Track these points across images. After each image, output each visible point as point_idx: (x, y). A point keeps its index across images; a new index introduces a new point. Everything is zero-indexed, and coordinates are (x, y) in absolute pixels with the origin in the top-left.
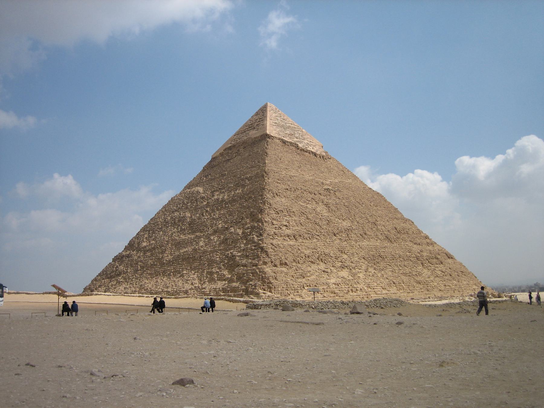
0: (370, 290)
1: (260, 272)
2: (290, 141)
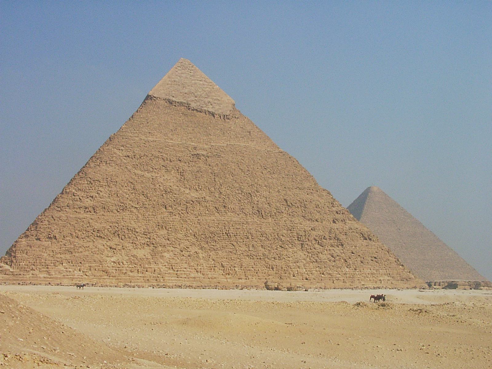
0: (171, 271)
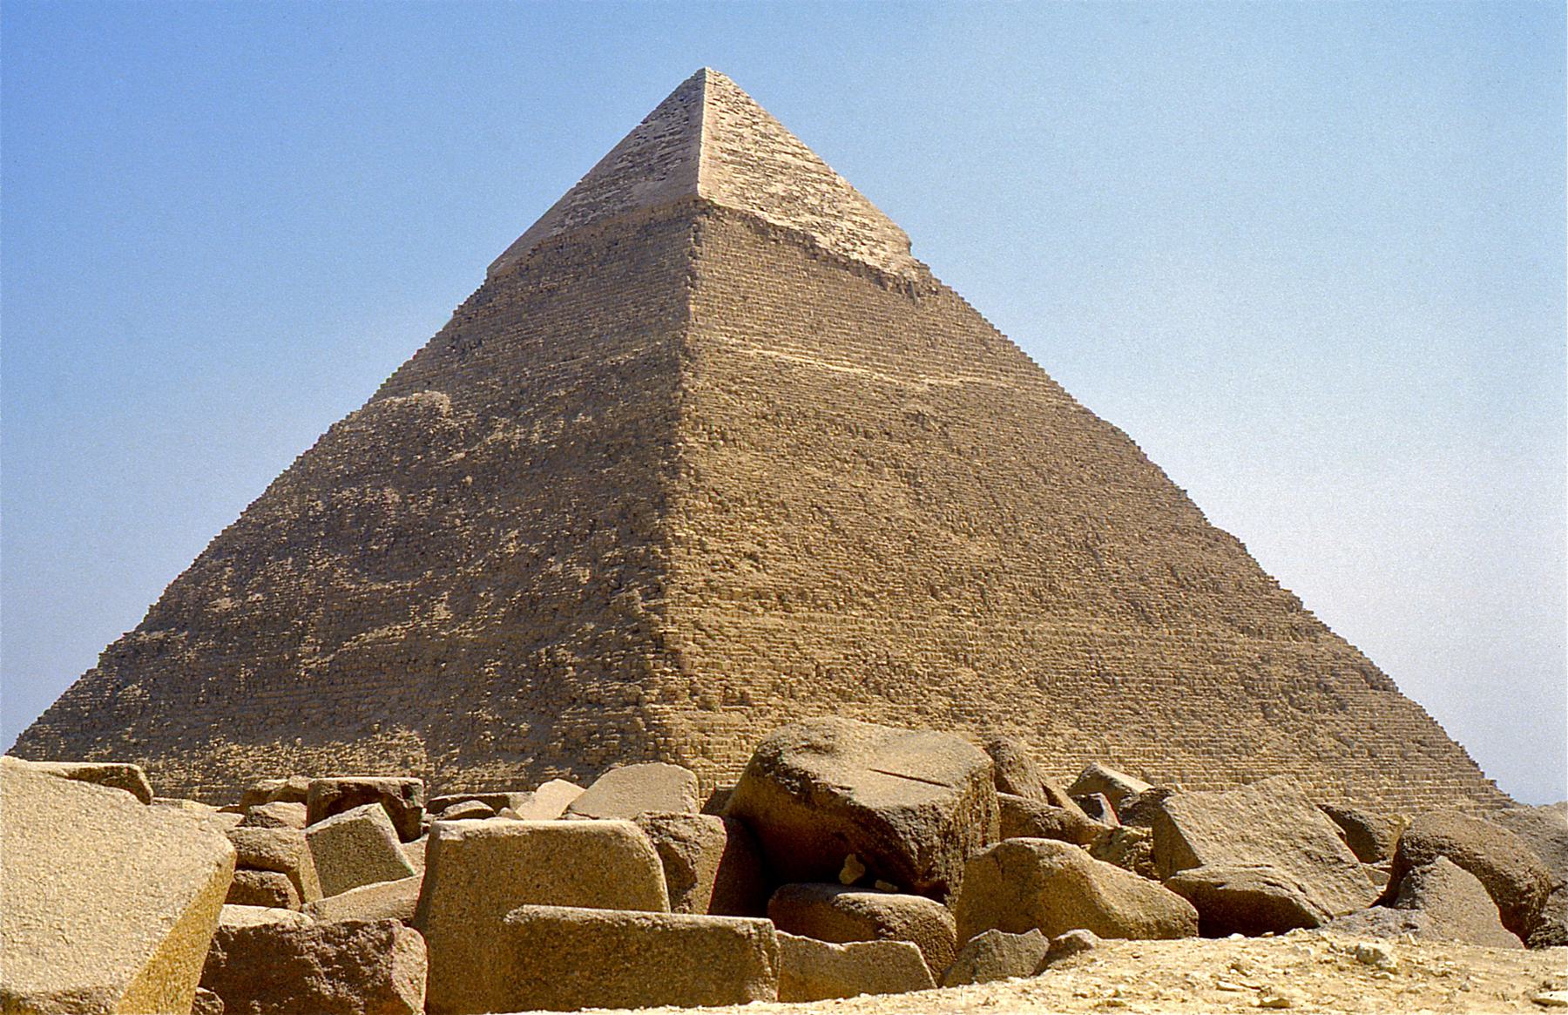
1: (647, 725)
2: (786, 223)
